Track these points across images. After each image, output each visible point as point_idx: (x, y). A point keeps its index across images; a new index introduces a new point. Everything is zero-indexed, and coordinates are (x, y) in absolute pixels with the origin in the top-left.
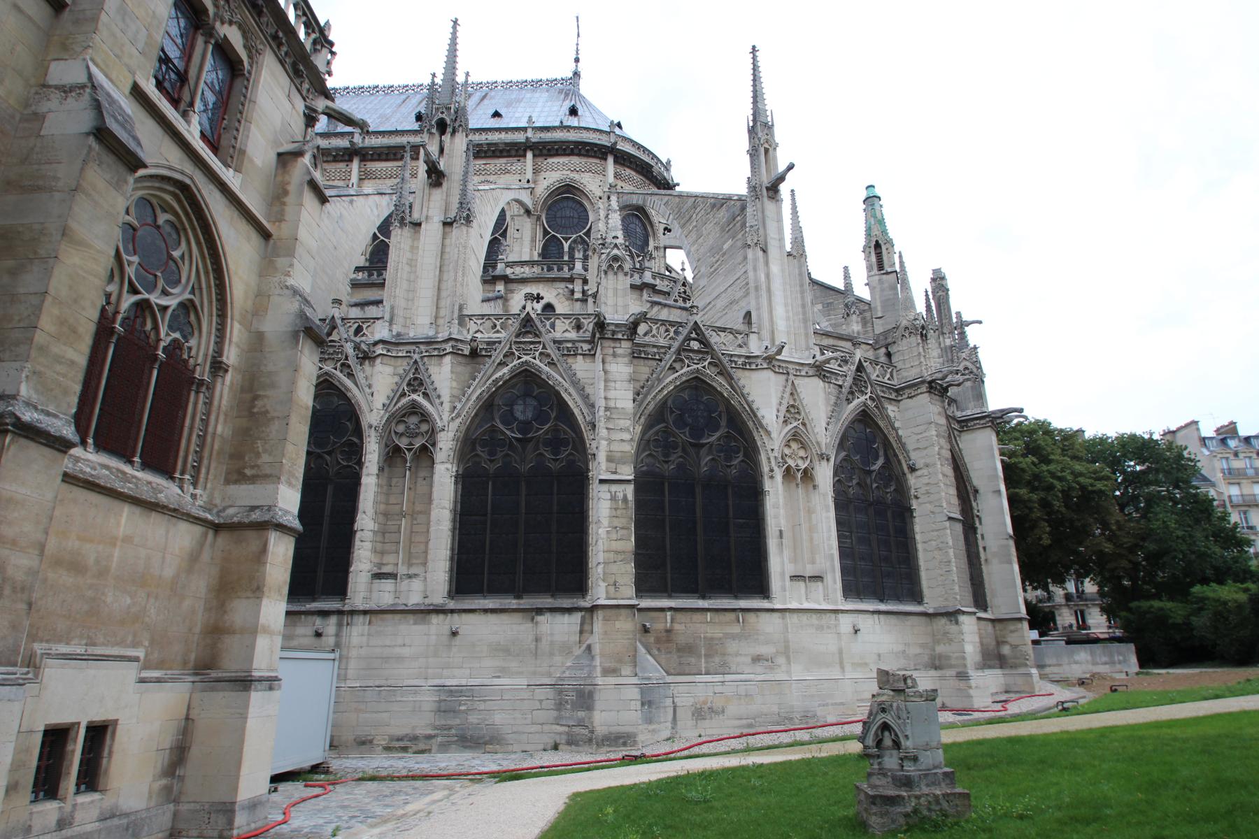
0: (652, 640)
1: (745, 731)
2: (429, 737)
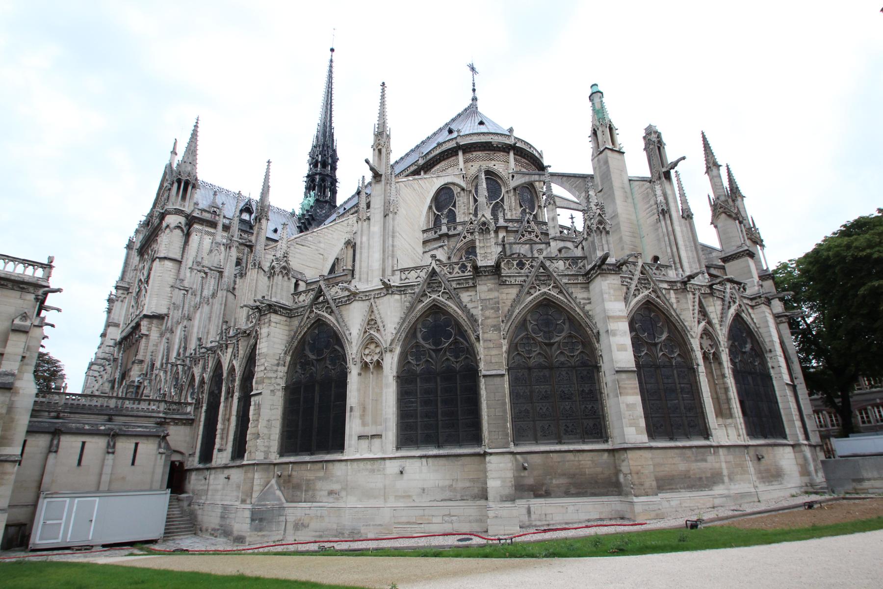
1: (318, 540)
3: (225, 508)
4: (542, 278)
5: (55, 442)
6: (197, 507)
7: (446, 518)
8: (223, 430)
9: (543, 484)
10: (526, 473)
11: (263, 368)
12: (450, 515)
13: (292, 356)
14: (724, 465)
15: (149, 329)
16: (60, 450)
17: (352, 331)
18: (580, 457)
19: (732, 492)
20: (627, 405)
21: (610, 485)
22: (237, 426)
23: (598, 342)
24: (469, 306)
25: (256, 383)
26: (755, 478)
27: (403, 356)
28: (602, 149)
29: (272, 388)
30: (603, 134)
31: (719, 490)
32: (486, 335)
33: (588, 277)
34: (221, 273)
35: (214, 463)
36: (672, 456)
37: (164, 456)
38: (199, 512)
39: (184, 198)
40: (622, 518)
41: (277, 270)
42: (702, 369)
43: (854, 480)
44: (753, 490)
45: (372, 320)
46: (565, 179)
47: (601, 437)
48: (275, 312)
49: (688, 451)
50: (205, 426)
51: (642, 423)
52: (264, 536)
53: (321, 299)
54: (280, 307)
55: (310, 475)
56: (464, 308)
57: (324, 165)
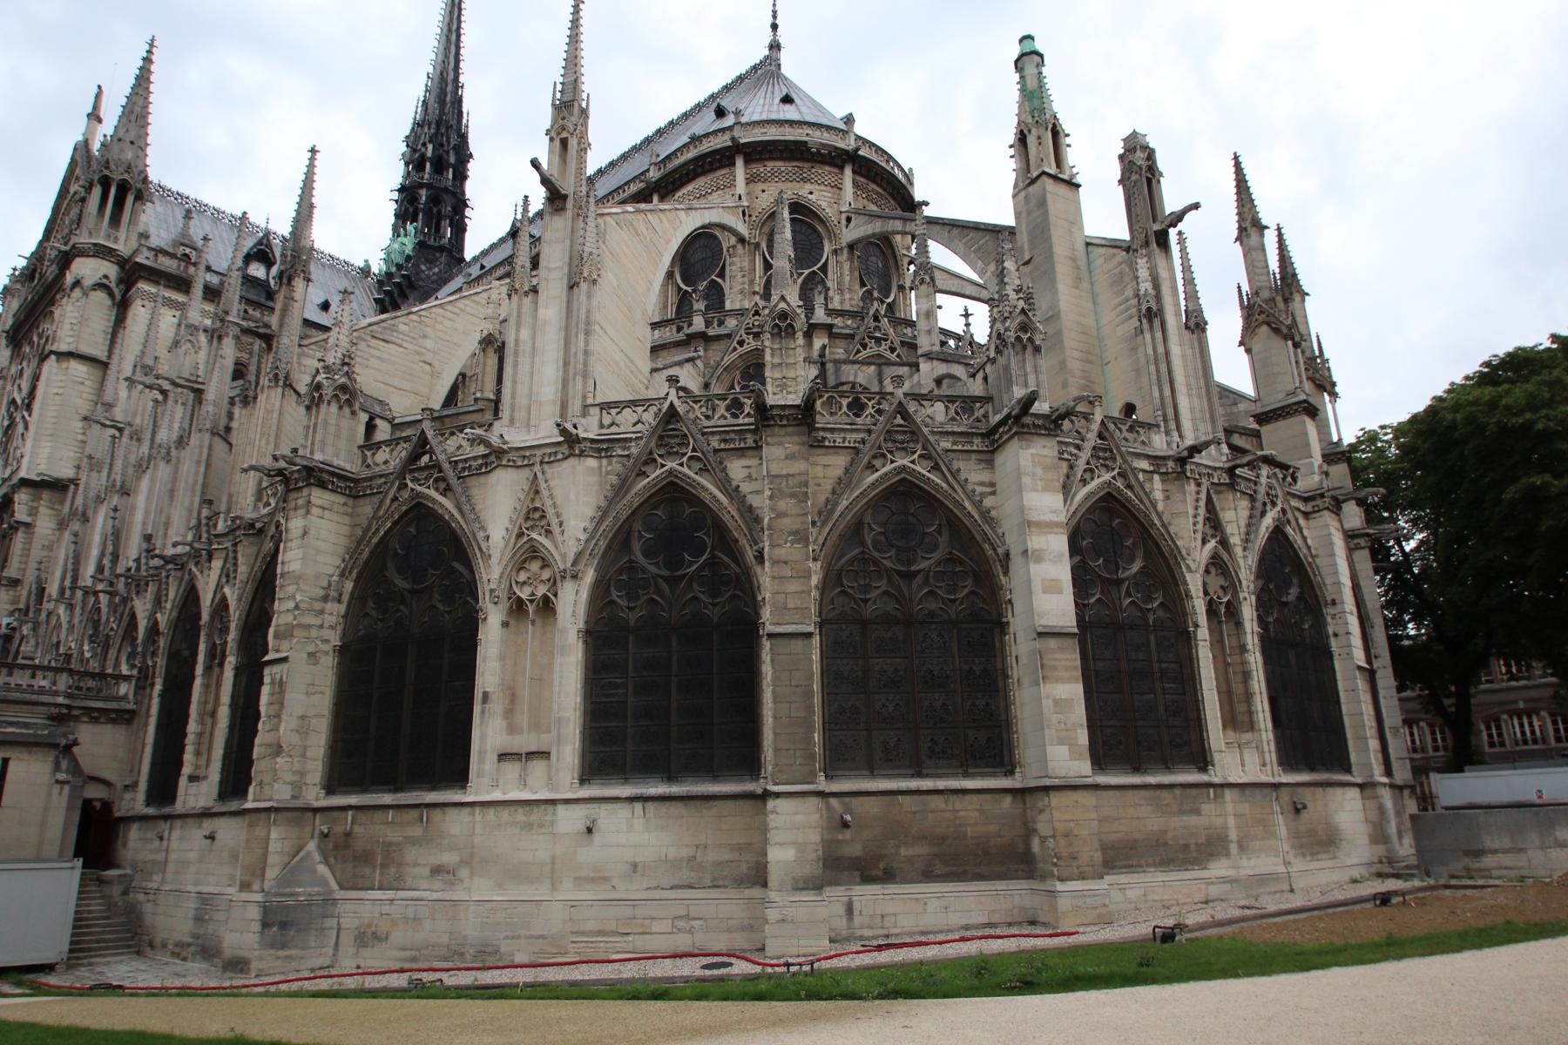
0: (331, 846)
1: (407, 966)
2: (189, 945)
3: (205, 900)
4: (900, 437)
6: (141, 897)
7: (681, 924)
8: (200, 735)
9: (880, 857)
10: (847, 835)
11: (291, 605)
12: (687, 917)
13: (357, 581)
14: (1231, 822)
15: (33, 512)
17: (490, 532)
18: (958, 803)
19: (1243, 872)
20: (1056, 702)
21: (1014, 858)
22: (232, 727)
23: (1006, 573)
24: (746, 488)
25: (276, 637)
26: (1286, 847)
27: (600, 591)
28: (1035, 174)
29: (311, 648)
30: (1039, 140)
31: (1219, 869)
32: (777, 551)
33: (992, 441)
34: (199, 393)
35: (179, 807)
36: (1135, 803)
37: (67, 788)
38: (148, 908)
39: (116, 220)
40: (1033, 923)
41: (328, 392)
42: (1203, 633)
43: (1467, 853)
44: (1281, 869)
45: (536, 509)
46: (956, 231)
47: (1001, 764)
48: (322, 485)
49: (1165, 794)
50: (159, 726)
51: (1083, 737)
52: (289, 957)
53: (426, 458)
54: (333, 474)
55: (393, 835)
56: (734, 493)
57: (439, 166)
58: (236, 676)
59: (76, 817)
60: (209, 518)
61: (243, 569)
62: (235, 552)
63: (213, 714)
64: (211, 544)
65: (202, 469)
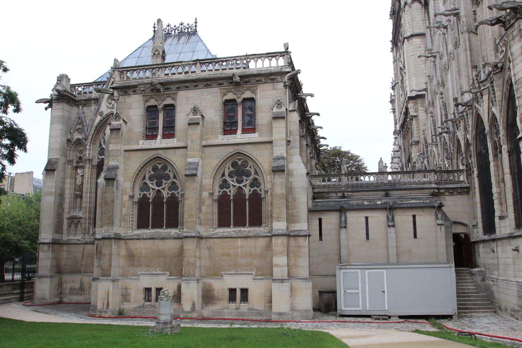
5: (343, 219)
8: (500, 193)
15: (416, 110)
16: (348, 226)
22: (514, 186)
34: (457, 15)
37: (443, 227)
38: (494, 288)
50: (481, 193)
58: (509, 156)
59: (452, 243)
60: (477, 76)
61: (498, 94)
62: (493, 86)
63: (503, 181)
64: (480, 87)
65: (468, 53)
